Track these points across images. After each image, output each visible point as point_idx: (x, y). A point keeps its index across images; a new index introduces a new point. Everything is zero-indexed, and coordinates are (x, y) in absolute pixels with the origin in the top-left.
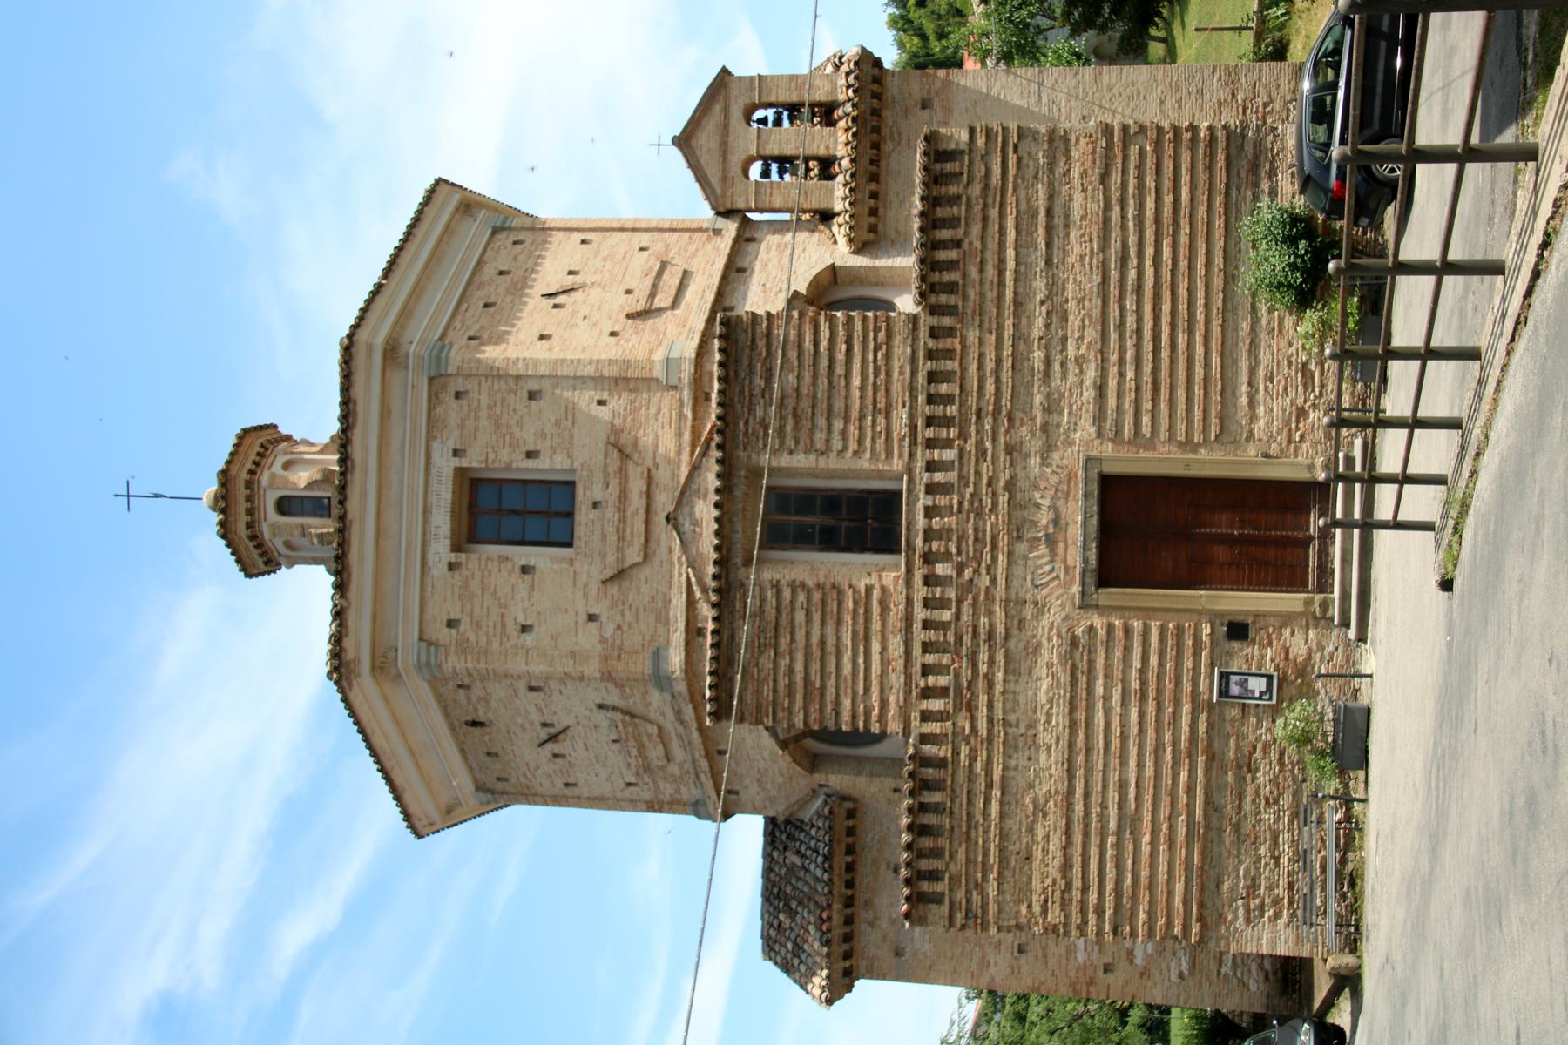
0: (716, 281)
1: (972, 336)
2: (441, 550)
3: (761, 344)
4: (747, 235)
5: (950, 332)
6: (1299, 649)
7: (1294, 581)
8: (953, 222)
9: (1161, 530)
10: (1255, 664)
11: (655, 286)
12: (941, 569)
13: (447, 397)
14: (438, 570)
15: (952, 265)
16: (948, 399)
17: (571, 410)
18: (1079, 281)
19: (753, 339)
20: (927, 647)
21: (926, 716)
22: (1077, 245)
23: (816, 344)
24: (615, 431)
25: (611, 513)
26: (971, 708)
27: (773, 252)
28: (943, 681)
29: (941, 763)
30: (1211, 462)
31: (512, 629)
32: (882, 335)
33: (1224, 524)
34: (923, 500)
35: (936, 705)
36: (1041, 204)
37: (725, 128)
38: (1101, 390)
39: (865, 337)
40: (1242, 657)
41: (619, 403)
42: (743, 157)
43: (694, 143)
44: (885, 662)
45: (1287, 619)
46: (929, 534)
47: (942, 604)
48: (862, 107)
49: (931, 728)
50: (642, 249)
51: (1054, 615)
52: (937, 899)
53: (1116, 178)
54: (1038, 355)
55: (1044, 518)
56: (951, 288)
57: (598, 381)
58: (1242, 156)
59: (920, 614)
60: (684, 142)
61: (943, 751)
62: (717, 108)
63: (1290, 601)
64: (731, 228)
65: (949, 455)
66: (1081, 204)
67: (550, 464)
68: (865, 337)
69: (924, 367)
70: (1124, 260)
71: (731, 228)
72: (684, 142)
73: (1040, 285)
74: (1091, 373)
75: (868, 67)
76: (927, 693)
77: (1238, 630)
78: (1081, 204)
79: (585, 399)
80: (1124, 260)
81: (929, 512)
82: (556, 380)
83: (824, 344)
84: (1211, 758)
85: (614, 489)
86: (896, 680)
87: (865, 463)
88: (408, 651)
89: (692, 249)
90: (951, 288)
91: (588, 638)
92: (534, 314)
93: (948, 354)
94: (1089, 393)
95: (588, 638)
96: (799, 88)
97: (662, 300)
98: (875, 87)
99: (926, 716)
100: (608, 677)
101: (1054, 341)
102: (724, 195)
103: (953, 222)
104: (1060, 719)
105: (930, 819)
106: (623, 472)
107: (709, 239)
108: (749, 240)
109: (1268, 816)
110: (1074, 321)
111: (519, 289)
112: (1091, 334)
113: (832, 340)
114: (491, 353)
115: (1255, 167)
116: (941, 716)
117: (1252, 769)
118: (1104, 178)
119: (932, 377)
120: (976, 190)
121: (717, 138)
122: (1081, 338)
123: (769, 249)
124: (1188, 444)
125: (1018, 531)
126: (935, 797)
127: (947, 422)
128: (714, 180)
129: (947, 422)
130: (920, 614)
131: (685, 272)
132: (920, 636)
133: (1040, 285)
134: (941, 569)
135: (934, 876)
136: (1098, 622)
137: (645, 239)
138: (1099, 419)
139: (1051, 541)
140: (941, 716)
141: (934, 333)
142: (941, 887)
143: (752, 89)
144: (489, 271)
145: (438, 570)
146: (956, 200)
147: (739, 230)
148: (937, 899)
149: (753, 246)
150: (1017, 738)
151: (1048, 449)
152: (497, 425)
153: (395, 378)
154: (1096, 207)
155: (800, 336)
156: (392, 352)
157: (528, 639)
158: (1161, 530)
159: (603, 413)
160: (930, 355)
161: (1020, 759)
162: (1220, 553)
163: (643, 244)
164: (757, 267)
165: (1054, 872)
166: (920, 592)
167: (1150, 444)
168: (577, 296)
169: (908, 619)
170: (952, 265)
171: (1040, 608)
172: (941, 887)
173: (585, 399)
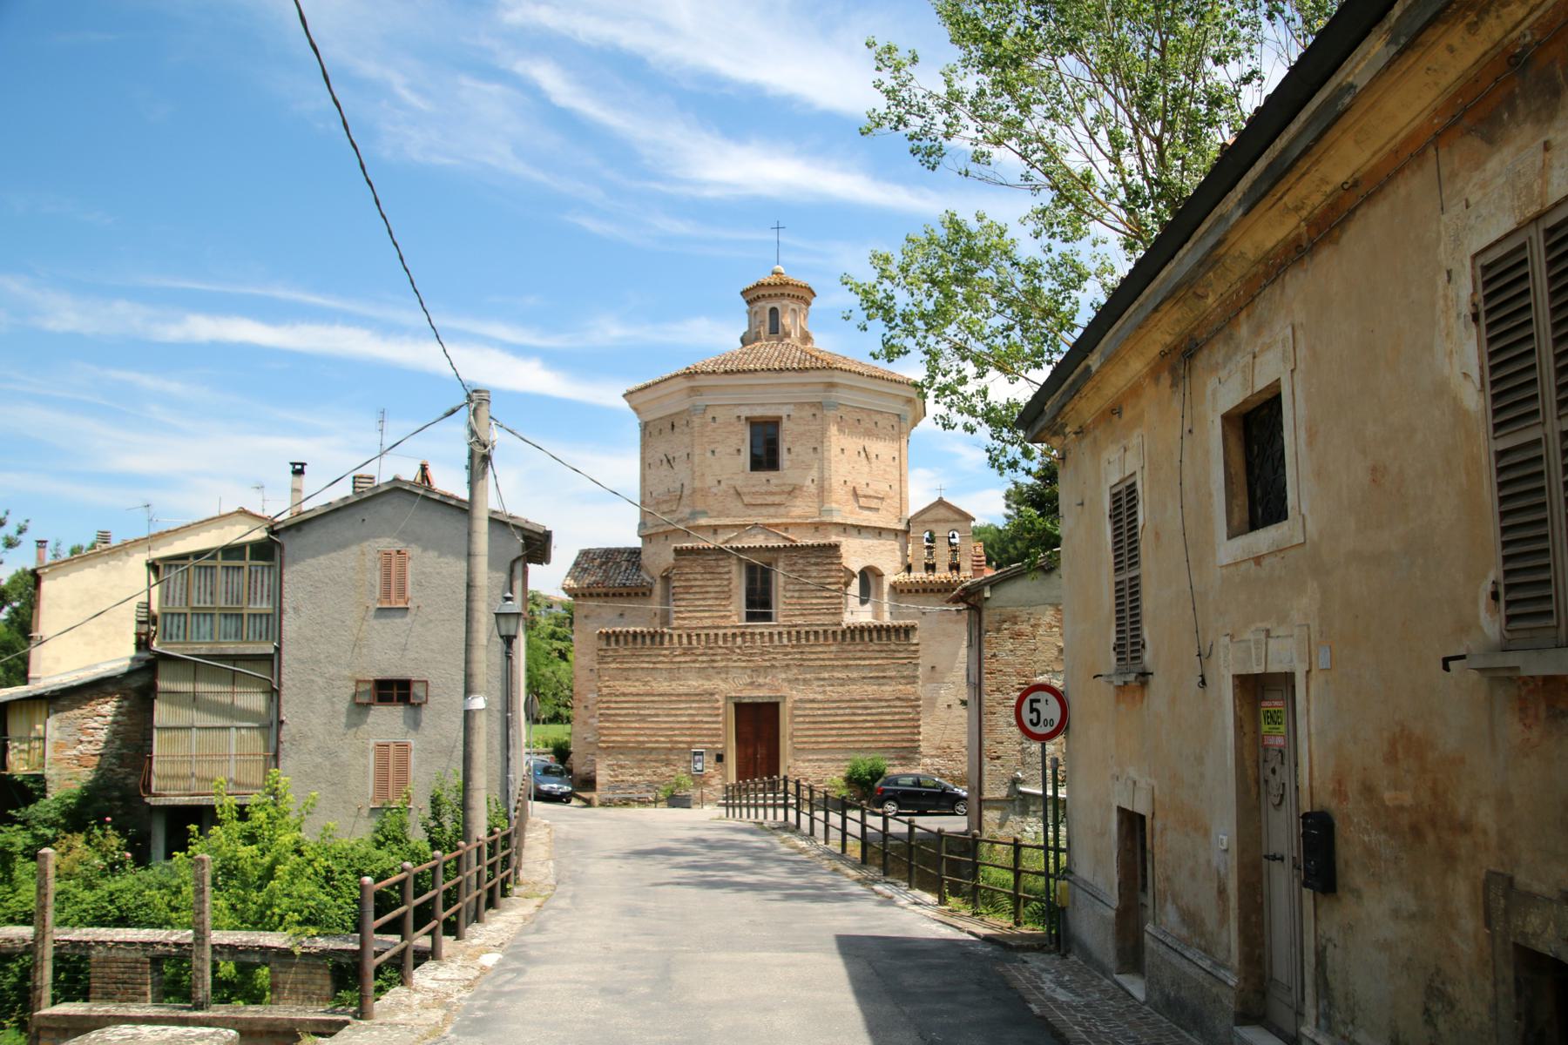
1: (833, 648)
2: (746, 412)
5: (835, 639)
6: (714, 782)
8: (880, 638)
9: (758, 727)
10: (707, 765)
12: (739, 640)
13: (814, 410)
14: (737, 412)
15: (862, 638)
16: (807, 640)
17: (809, 467)
18: (856, 690)
20: (707, 635)
21: (680, 636)
22: (871, 689)
24: (801, 488)
25: (764, 489)
26: (684, 654)
28: (694, 643)
29: (662, 643)
30: (786, 745)
31: (713, 447)
33: (762, 752)
34: (766, 631)
35: (685, 640)
36: (888, 674)
37: (947, 521)
38: (813, 701)
40: (709, 760)
41: (813, 489)
44: (701, 618)
45: (725, 777)
46: (753, 634)
47: (725, 641)
49: (676, 639)
51: (723, 686)
52: (608, 644)
53: (898, 703)
54: (826, 675)
55: (761, 680)
56: (853, 638)
57: (822, 479)
58: (909, 752)
59: (721, 632)
61: (666, 644)
63: (732, 778)
65: (785, 641)
66: (888, 690)
67: (784, 458)
69: (821, 630)
70: (866, 708)
71: (902, 527)
73: (855, 675)
74: (820, 697)
76: (689, 636)
77: (720, 758)
78: (888, 690)
79: (814, 474)
80: (866, 708)
81: (761, 634)
82: (822, 460)
84: (670, 749)
85: (774, 489)
86: (694, 623)
87: (781, 606)
88: (700, 401)
90: (853, 638)
91: (710, 481)
92: (853, 443)
93: (826, 638)
94: (811, 696)
95: (710, 481)
97: (862, 501)
99: (680, 636)
100: (694, 491)
101: (832, 682)
103: (880, 638)
104: (682, 690)
105: (639, 639)
106: (783, 492)
109: (649, 772)
110: (840, 689)
111: (868, 434)
112: (835, 696)
114: (833, 429)
115: (904, 758)
116: (680, 643)
117: (667, 765)
118: (898, 699)
119: (816, 633)
120: (893, 647)
122: (834, 692)
124: (792, 736)
125: (755, 670)
126: (648, 641)
127: (798, 639)
129: (798, 639)
130: (721, 632)
132: (712, 632)
133: (855, 675)
134: (739, 640)
135: (617, 642)
136: (721, 703)
137: (896, 487)
138: (801, 701)
139: (752, 683)
140: (680, 643)
141: (834, 633)
142: (613, 645)
144: (877, 417)
145: (737, 412)
146: (889, 638)
148: (608, 644)
150: (673, 673)
151: (789, 681)
152: (802, 434)
153: (821, 387)
154: (887, 696)
156: (831, 385)
157: (709, 454)
158: (758, 727)
159: (808, 482)
160: (825, 632)
161: (665, 674)
162: (750, 751)
165: (623, 690)
166: (730, 632)
167: (792, 722)
168: (865, 462)
169: (718, 627)
170: (862, 638)
171: (725, 680)
172: (613, 645)
173: (814, 474)
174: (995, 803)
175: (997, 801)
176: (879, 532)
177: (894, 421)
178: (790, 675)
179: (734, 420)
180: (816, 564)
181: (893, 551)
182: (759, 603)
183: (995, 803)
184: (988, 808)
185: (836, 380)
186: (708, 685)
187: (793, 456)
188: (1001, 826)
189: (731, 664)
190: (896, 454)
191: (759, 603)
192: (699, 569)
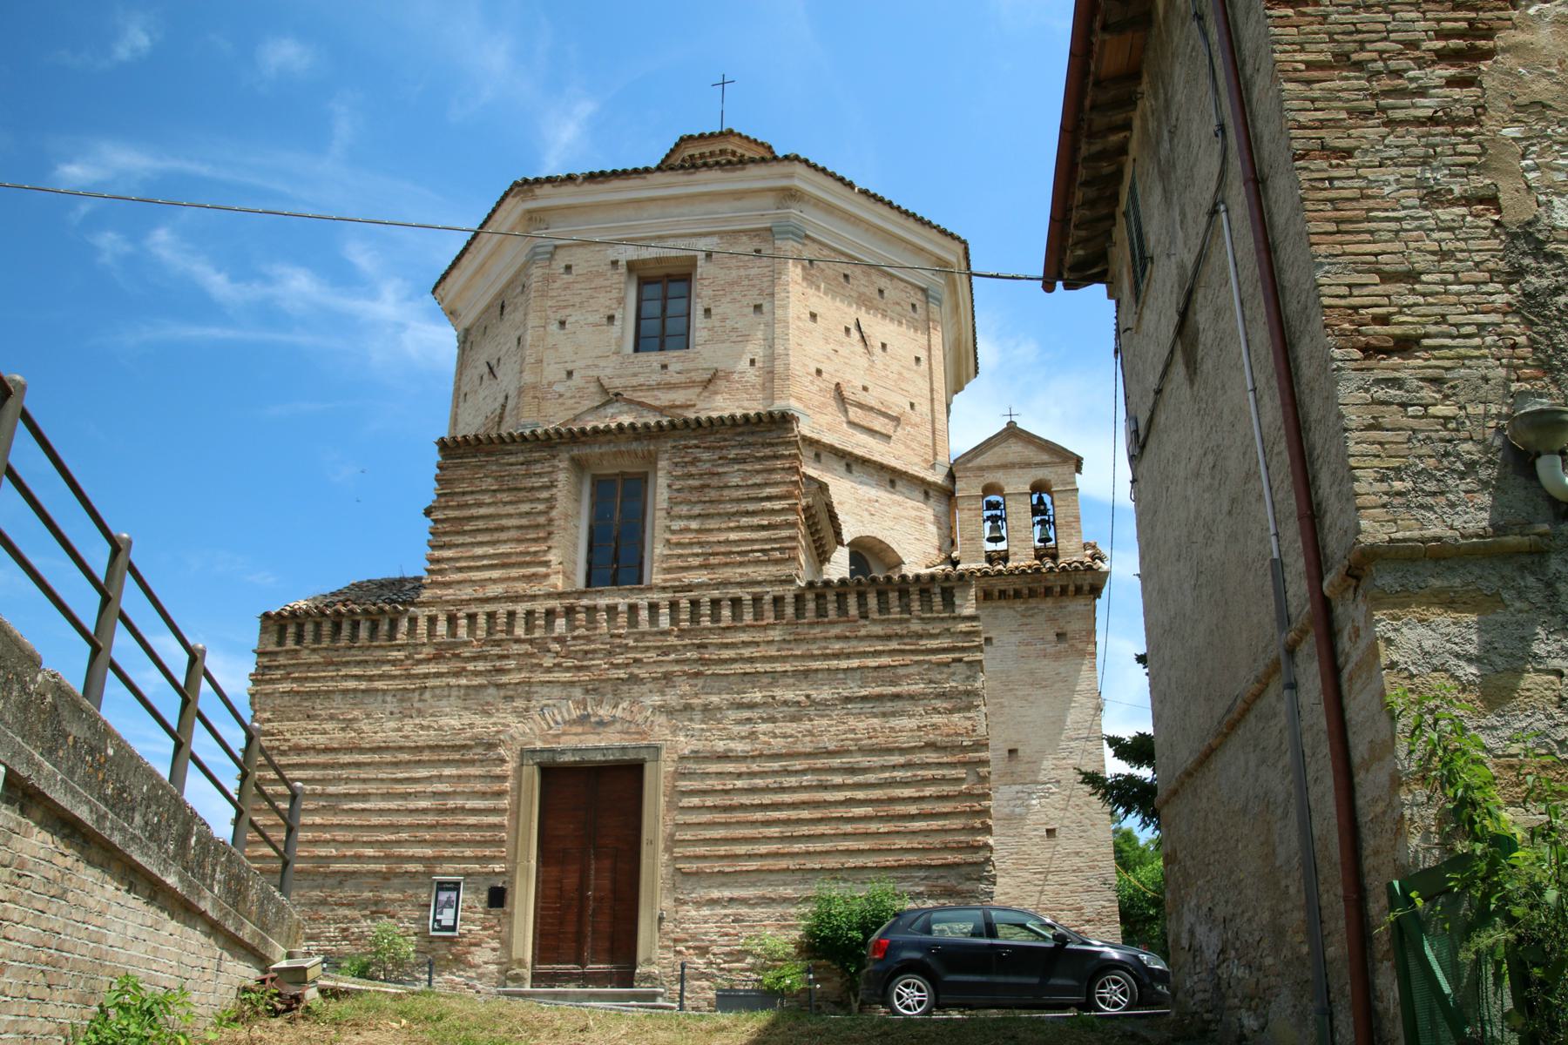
0: (877, 458)
1: (775, 634)
2: (629, 253)
3: (768, 451)
4: (931, 493)
5: (779, 615)
6: (480, 956)
7: (546, 946)
8: (884, 608)
10: (465, 913)
11: (871, 409)
12: (560, 624)
13: (756, 244)
14: (612, 253)
15: (842, 609)
16: (716, 617)
17: (745, 338)
18: (829, 730)
19: (772, 445)
20: (491, 616)
21: (432, 620)
22: (864, 725)
23: (769, 498)
24: (728, 376)
25: (656, 378)
26: (436, 658)
27: (914, 513)
28: (462, 633)
29: (392, 636)
30: (656, 864)
31: (560, 315)
32: (777, 555)
33: (599, 882)
34: (622, 603)
35: (442, 628)
36: (903, 688)
37: (1028, 465)
38: (724, 757)
39: (775, 540)
40: (472, 899)
41: (752, 375)
42: (1002, 483)
43: (1012, 440)
44: (483, 583)
45: (506, 944)
46: (592, 610)
47: (529, 628)
48: (1051, 577)
49: (422, 625)
50: (912, 405)
51: (516, 727)
52: (281, 641)
53: (932, 757)
54: (758, 696)
55: (604, 712)
56: (821, 612)
57: (772, 358)
59: (521, 608)
60: (1012, 432)
61: (401, 637)
62: (1045, 457)
63: (524, 944)
64: (938, 477)
65: (664, 622)
66: (906, 727)
67: (700, 327)
68: (775, 540)
69: (745, 595)
70: (852, 771)
71: (938, 477)
72: (1012, 432)
73: (825, 693)
74: (739, 747)
75: (1087, 580)
76: (452, 620)
77: (497, 898)
78: (906, 727)
79: (756, 349)
80: (852, 771)
81: (612, 610)
82: (770, 325)
83: (768, 505)
84: (385, 877)
85: (676, 379)
86: (467, 592)
87: (659, 550)
88: (545, 237)
89: (914, 445)
90: (821, 612)
91: (553, 372)
92: (838, 311)
93: (758, 615)
94: (720, 746)
95: (553, 372)
96: (1068, 524)
97: (855, 414)
98: (1071, 588)
99: (432, 620)
100: (521, 391)
101: (771, 710)
102: (967, 469)
103: (884, 608)
104: (424, 738)
105: (346, 630)
106: (691, 384)
107: (926, 461)
108: (927, 494)
109: (332, 931)
110: (791, 728)
111: (863, 301)
112: (778, 745)
113: (773, 512)
114: (794, 272)
115: (949, 893)
116: (431, 633)
117: (374, 916)
118: (932, 746)
119: (736, 603)
120: (916, 626)
121: (1017, 459)
122: (774, 735)
123: (918, 509)
124: (672, 842)
125: (594, 690)
126: (363, 633)
127: (695, 617)
128: (979, 461)
129: (695, 617)
130: (521, 608)
131: (889, 437)
132: (502, 609)
133: (825, 693)
134: (560, 624)
135: (299, 638)
136: (509, 767)
138: (696, 756)
139: (583, 720)
140: (431, 633)
141: (778, 601)
142: (290, 644)
143: (1065, 483)
144: (883, 282)
145: (612, 253)
146: (906, 608)
147: (935, 484)
148: (281, 641)
149: (922, 497)
150: (408, 699)
151: (669, 711)
152: (732, 284)
153: (769, 200)
154: (904, 740)
155: (776, 484)
156: (790, 195)
157: (554, 327)
159: (744, 364)
160: (757, 600)
161: (392, 704)
162: (571, 881)
163: (917, 407)
164: (895, 497)
165: (296, 739)
166: (540, 607)
167: (672, 806)
168: (860, 348)
169: (517, 598)
170: (842, 609)
171: (523, 714)
172: (290, 644)
173: (756, 349)
174: (1422, 570)
175: (1438, 555)
176: (892, 477)
177: (917, 298)
178: (672, 698)
179: (606, 268)
180: (735, 461)
181: (920, 521)
182: (615, 556)
183: (1422, 570)
184: (1401, 599)
185: (797, 183)
186: (482, 725)
187: (715, 320)
188: (1497, 692)
189: (539, 676)
190: (923, 355)
191: (615, 556)
192: (489, 484)
